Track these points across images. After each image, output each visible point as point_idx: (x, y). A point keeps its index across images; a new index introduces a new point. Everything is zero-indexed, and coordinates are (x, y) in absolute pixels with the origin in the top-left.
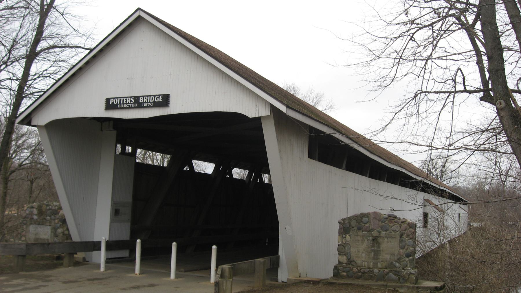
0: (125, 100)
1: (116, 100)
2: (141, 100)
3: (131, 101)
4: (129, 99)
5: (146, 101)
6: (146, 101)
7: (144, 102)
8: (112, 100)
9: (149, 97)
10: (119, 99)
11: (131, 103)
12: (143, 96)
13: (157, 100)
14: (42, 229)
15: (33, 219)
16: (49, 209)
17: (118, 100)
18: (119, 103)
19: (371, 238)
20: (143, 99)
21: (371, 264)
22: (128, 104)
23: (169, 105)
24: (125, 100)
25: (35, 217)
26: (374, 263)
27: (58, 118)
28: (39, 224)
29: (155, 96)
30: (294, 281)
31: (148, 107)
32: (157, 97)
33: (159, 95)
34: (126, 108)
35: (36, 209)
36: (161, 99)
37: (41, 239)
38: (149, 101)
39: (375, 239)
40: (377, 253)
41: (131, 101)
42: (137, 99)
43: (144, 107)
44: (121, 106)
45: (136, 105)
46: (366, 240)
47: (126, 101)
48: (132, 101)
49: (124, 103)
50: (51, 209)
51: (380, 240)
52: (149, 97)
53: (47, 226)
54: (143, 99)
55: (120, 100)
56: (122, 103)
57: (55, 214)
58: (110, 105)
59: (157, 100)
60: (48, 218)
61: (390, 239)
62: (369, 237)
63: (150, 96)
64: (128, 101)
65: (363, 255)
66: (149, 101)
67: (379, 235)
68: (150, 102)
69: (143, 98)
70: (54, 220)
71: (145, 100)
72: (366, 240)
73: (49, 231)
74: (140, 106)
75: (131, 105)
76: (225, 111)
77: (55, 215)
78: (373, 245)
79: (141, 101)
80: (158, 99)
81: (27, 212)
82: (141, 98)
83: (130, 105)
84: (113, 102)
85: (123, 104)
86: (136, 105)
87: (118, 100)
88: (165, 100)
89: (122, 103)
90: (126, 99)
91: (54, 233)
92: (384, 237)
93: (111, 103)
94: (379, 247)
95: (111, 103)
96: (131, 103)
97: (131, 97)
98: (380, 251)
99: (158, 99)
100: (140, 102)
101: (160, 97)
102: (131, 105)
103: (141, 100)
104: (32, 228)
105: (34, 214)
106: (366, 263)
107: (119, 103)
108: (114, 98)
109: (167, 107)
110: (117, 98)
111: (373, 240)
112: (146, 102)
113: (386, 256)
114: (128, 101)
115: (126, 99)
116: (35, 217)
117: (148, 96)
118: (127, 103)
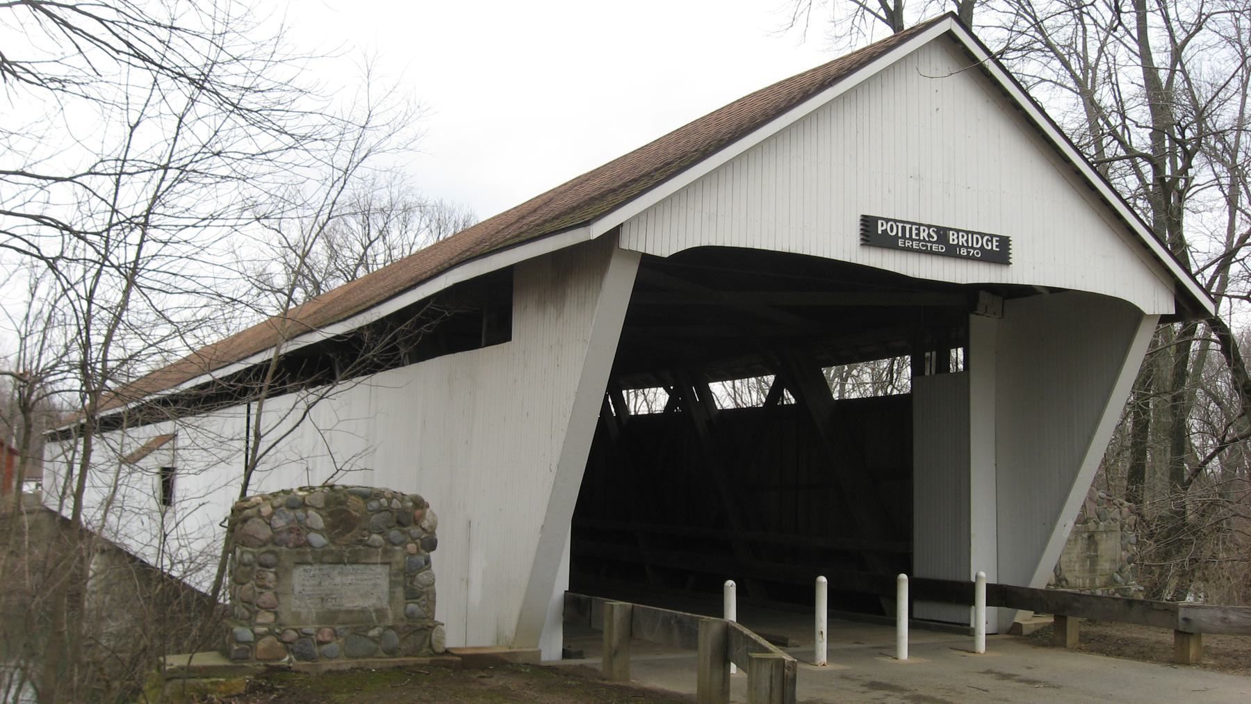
0: (914, 232)
1: (892, 226)
2: (953, 238)
3: (929, 235)
4: (924, 231)
5: (965, 245)
6: (965, 245)
7: (961, 244)
8: (882, 225)
9: (970, 235)
10: (900, 225)
11: (930, 242)
12: (958, 231)
13: (988, 245)
14: (350, 577)
15: (308, 544)
16: (379, 511)
17: (897, 226)
18: (900, 235)
19: (1085, 535)
20: (958, 237)
21: (1088, 581)
22: (922, 241)
23: (1011, 261)
24: (914, 232)
25: (317, 539)
26: (1091, 580)
27: (714, 241)
28: (339, 562)
29: (982, 235)
30: (1033, 626)
31: (969, 258)
32: (988, 240)
33: (992, 236)
34: (919, 251)
35: (317, 509)
36: (997, 246)
37: (350, 612)
38: (970, 245)
39: (1091, 537)
40: (1094, 560)
41: (929, 235)
42: (942, 233)
43: (960, 257)
44: (907, 244)
45: (942, 248)
46: (1080, 538)
47: (918, 234)
48: (933, 238)
49: (914, 237)
50: (389, 509)
51: (1097, 537)
52: (970, 235)
53: (373, 567)
54: (958, 237)
55: (904, 229)
56: (908, 236)
57: (404, 526)
58: (871, 232)
59: (988, 245)
60: (376, 538)
61: (1109, 534)
62: (1085, 532)
63: (973, 233)
64: (924, 235)
65: (1077, 566)
66: (970, 245)
67: (1098, 528)
68: (972, 247)
69: (956, 235)
70: (403, 544)
71: (962, 241)
72: (1080, 538)
73: (384, 584)
74: (952, 253)
75: (931, 247)
76: (1108, 294)
77: (406, 529)
78: (1088, 549)
79: (953, 240)
80: (990, 244)
81: (279, 523)
82: (953, 235)
83: (929, 245)
84: (886, 229)
85: (911, 238)
86: (942, 248)
87: (897, 226)
88: (1000, 253)
89: (908, 236)
90: (916, 229)
91: (405, 587)
92: (1102, 532)
93: (880, 232)
94: (1096, 550)
95: (880, 232)
96: (930, 242)
97: (929, 227)
98: (1097, 556)
99: (990, 244)
100: (951, 242)
101: (994, 239)
102: (931, 247)
103: (953, 238)
104: (302, 579)
105: (311, 529)
106: (1081, 580)
107: (900, 235)
108: (887, 220)
109: (1005, 266)
110: (895, 221)
111: (1089, 537)
112: (965, 247)
113: (1105, 565)
114: (924, 235)
115: (918, 229)
116: (317, 539)
117: (967, 232)
118: (922, 238)
